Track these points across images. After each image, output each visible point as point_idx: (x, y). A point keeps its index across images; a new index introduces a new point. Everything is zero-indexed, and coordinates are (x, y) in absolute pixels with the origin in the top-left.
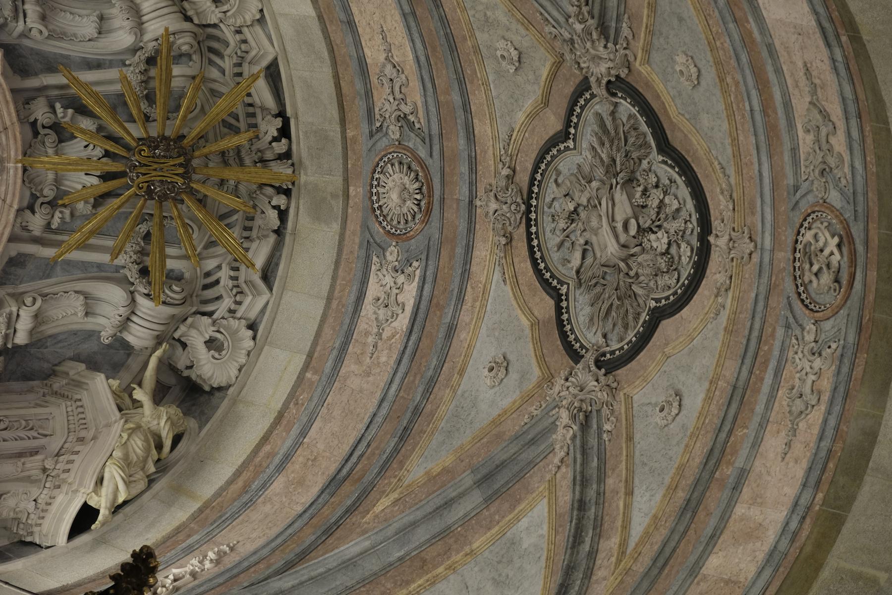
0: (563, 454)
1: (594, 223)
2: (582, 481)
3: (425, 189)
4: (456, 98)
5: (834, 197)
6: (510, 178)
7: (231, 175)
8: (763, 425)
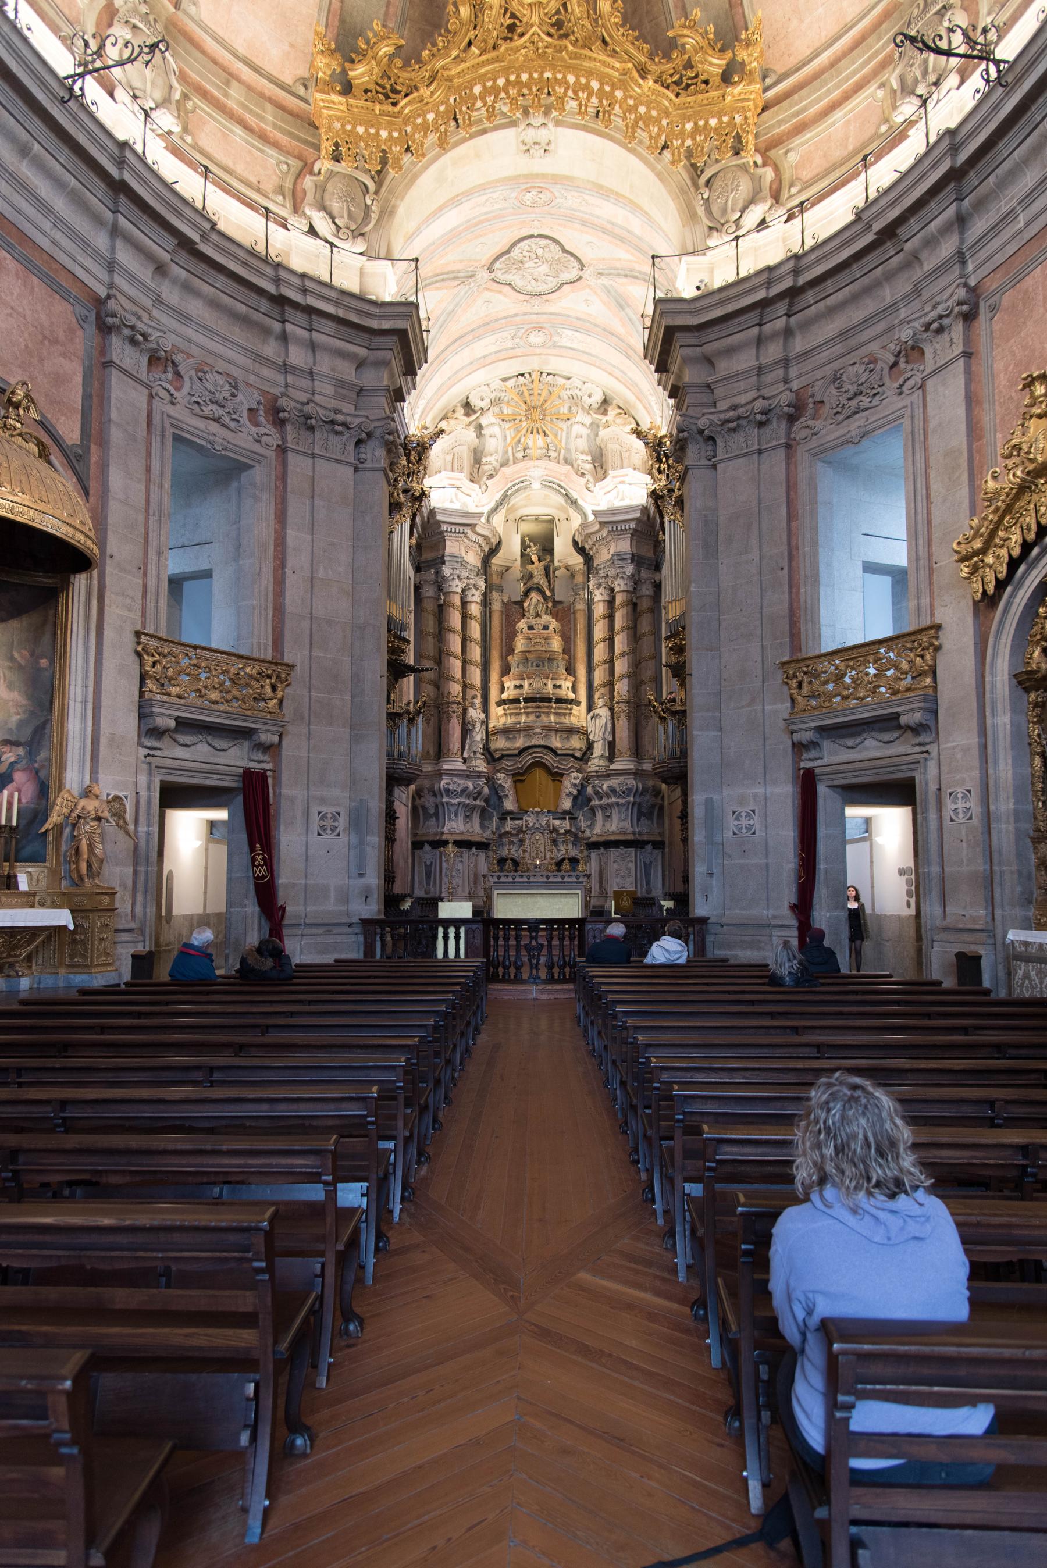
2: (619, 275)
3: (535, 329)
4: (503, 321)
5: (514, 195)
7: (536, 393)
8: (591, 214)
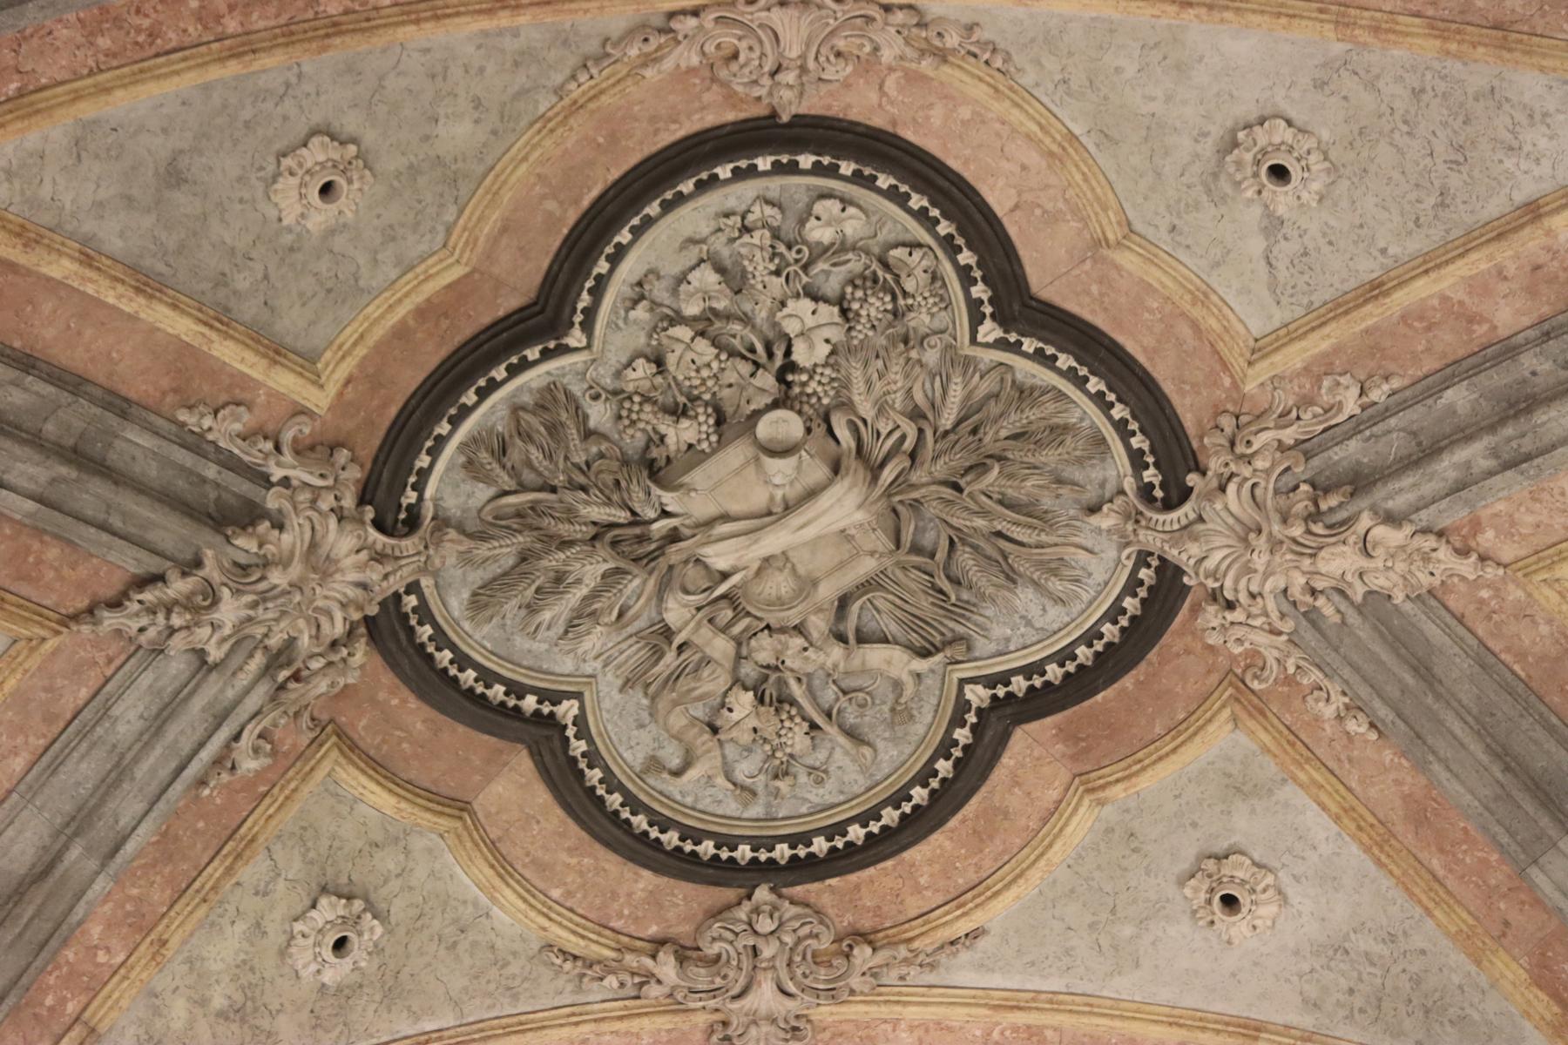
0: (1444, 553)
1: (779, 584)
6: (685, 954)
